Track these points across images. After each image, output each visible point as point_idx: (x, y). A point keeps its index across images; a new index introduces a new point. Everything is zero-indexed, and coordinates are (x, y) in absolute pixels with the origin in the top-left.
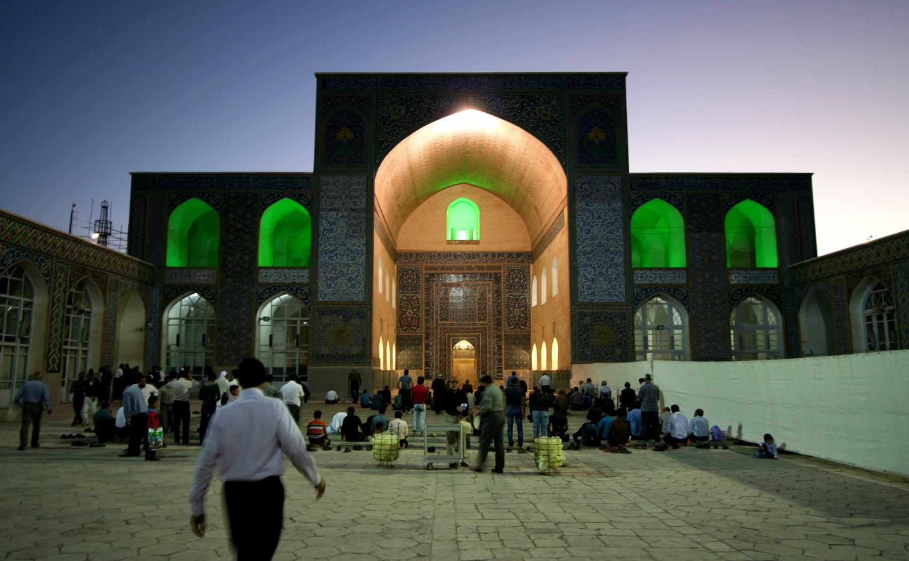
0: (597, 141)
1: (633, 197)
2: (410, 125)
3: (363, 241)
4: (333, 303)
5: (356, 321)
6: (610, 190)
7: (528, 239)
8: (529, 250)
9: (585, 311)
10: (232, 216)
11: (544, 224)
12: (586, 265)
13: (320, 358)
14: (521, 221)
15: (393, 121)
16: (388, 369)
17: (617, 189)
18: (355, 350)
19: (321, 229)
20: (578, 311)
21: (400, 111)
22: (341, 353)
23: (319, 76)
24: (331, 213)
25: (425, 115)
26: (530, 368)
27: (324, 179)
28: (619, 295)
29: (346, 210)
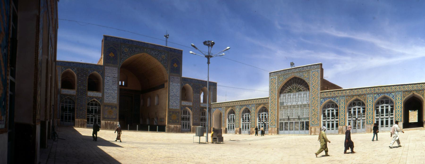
27: (106, 67)
28: (178, 108)
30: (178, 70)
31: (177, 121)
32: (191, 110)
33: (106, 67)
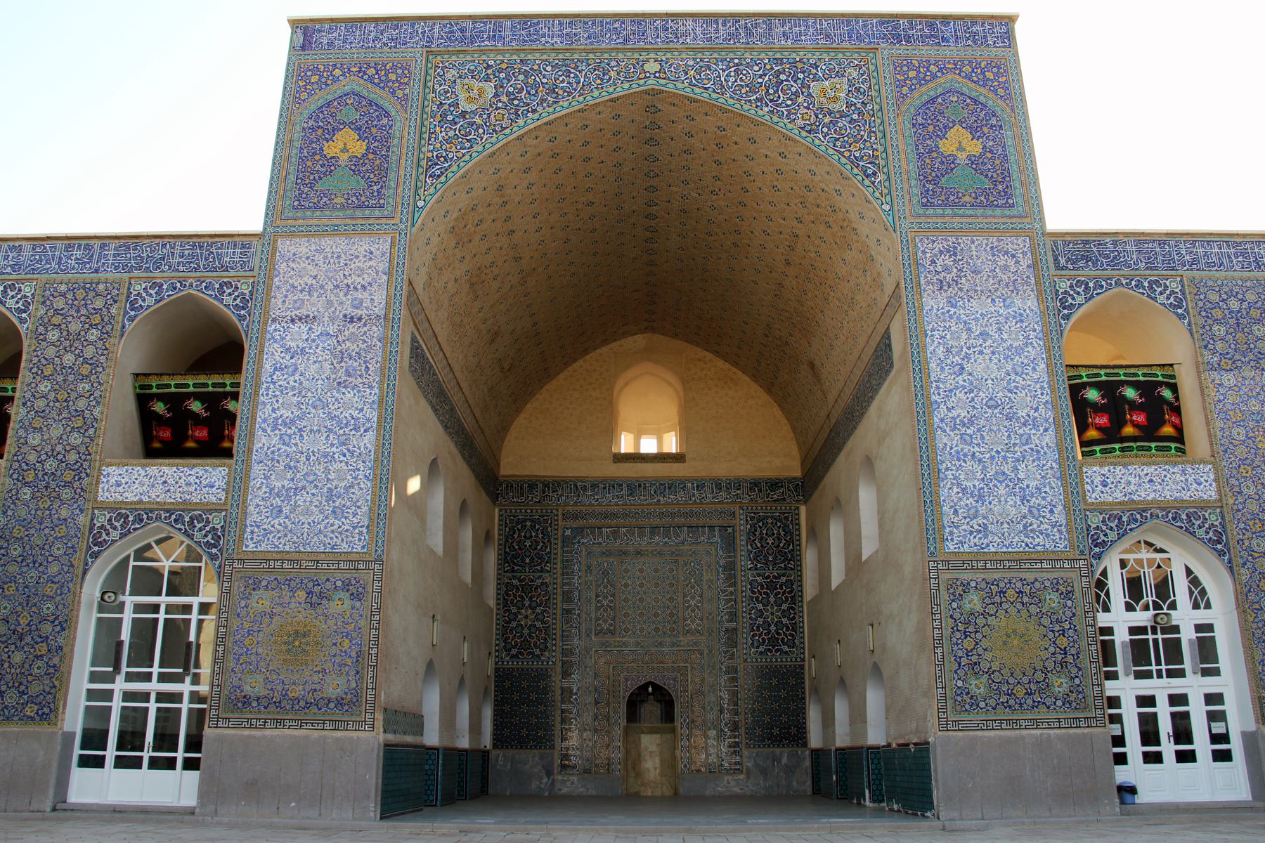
0: (962, 158)
1: (1064, 286)
2: (505, 123)
3: (373, 395)
4: (283, 557)
5: (340, 605)
6: (1006, 268)
7: (795, 452)
8: (797, 473)
9: (965, 576)
10: (53, 335)
11: (831, 398)
12: (960, 457)
13: (241, 706)
14: (776, 411)
15: (464, 113)
16: (464, 743)
17: (1025, 262)
18: (335, 686)
19: (268, 366)
20: (945, 576)
21: (481, 92)
22: (296, 692)
23: (295, 24)
24: (295, 328)
25: (543, 101)
26: (805, 745)
27: (284, 245)
28: (1051, 534)
29: (332, 319)
30: (1001, 180)
31: (1060, 684)
32: (1218, 543)
33: (284, 245)
